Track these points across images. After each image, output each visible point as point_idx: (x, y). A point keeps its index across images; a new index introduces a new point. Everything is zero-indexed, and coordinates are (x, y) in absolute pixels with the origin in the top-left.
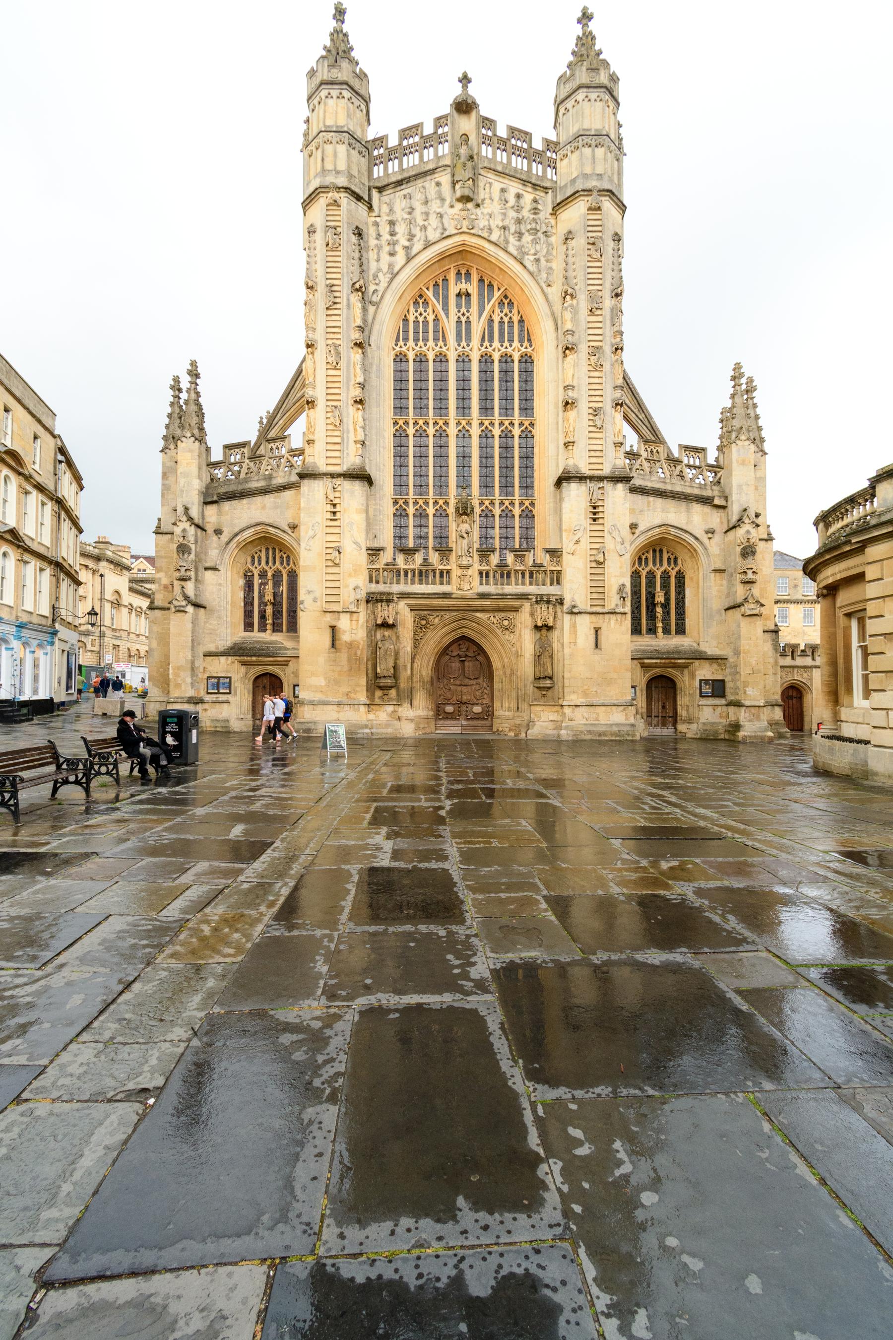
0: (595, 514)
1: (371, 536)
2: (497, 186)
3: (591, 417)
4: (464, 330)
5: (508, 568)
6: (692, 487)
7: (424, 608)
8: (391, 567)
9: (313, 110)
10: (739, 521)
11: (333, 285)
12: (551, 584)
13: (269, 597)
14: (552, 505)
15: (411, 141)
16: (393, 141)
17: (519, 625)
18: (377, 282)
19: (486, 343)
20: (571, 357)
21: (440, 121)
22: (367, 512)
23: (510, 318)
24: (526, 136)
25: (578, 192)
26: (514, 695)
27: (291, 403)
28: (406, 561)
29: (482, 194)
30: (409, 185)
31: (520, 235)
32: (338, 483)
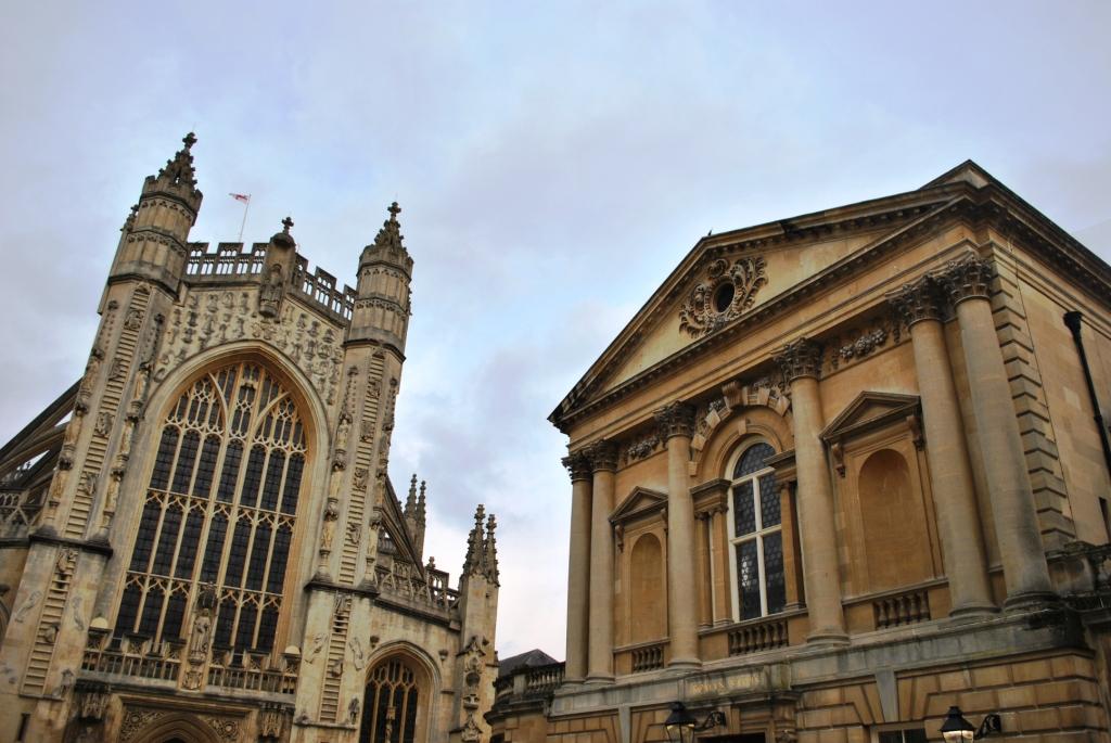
0: (338, 624)
3: (349, 532)
4: (242, 421)
6: (433, 608)
7: (141, 703)
9: (144, 207)
10: (469, 647)
14: (298, 607)
15: (229, 254)
16: (212, 250)
19: (261, 437)
20: (339, 474)
21: (257, 246)
23: (289, 419)
24: (332, 280)
25: (366, 340)
27: (30, 442)
29: (283, 314)
31: (311, 356)
32: (75, 553)
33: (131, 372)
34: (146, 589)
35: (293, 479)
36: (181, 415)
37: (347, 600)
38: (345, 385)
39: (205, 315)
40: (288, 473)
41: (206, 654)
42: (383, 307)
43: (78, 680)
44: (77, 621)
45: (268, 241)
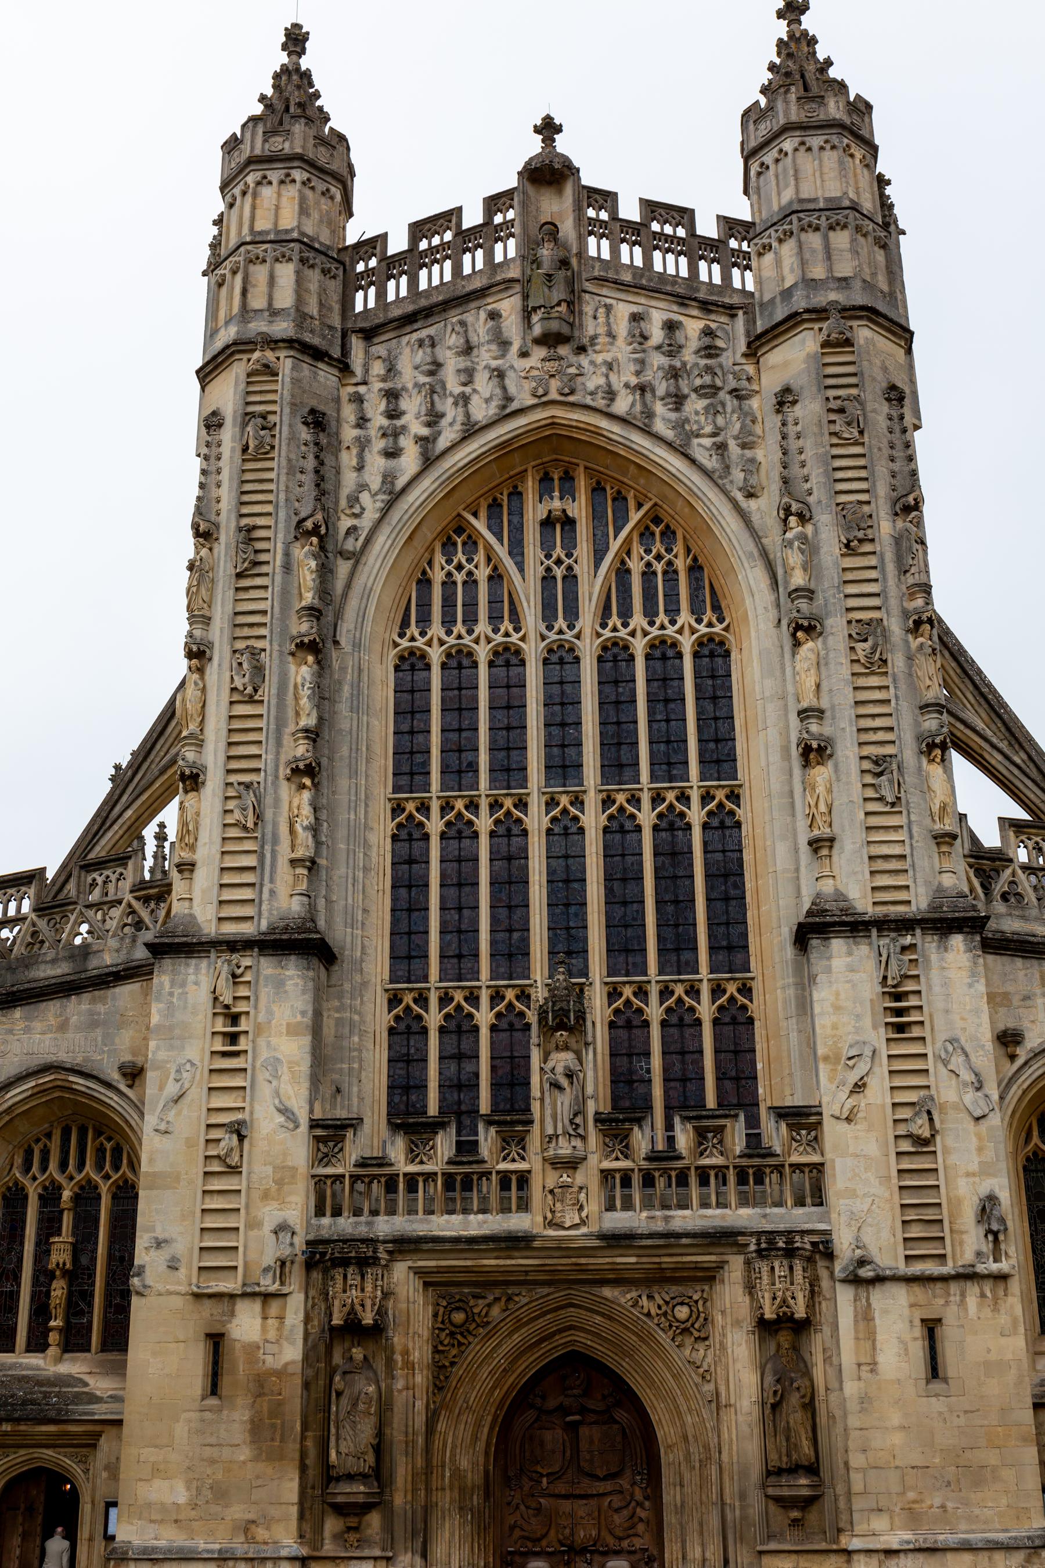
0: (899, 1012)
1: (327, 1090)
2: (623, 311)
3: (869, 779)
5: (679, 1164)
8: (376, 1171)
11: (255, 527)
12: (800, 1202)
13: (60, 1255)
14: (791, 992)
15: (436, 241)
16: (398, 244)
17: (719, 1318)
18: (357, 510)
19: (615, 620)
21: (494, 203)
22: (316, 1030)
23: (670, 563)
24: (684, 215)
25: (796, 314)
26: (714, 1521)
27: (155, 769)
28: (412, 1156)
29: (591, 327)
30: (431, 321)
31: (678, 400)
32: (247, 962)
33: (280, 546)
34: (434, 1018)
35: (714, 698)
36: (424, 620)
37: (904, 949)
38: (773, 440)
39: (416, 385)
40: (698, 688)
41: (583, 1138)
42: (817, 229)
43: (308, 1243)
44: (279, 1111)
45: (512, 182)
